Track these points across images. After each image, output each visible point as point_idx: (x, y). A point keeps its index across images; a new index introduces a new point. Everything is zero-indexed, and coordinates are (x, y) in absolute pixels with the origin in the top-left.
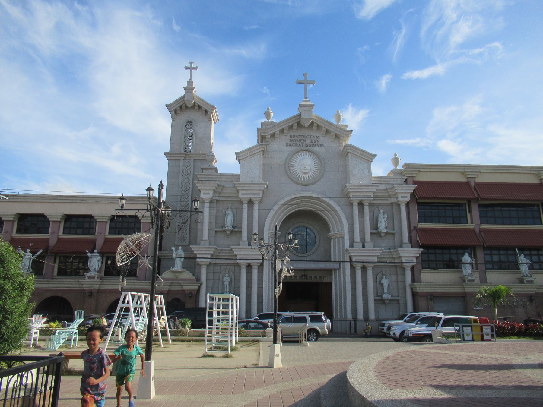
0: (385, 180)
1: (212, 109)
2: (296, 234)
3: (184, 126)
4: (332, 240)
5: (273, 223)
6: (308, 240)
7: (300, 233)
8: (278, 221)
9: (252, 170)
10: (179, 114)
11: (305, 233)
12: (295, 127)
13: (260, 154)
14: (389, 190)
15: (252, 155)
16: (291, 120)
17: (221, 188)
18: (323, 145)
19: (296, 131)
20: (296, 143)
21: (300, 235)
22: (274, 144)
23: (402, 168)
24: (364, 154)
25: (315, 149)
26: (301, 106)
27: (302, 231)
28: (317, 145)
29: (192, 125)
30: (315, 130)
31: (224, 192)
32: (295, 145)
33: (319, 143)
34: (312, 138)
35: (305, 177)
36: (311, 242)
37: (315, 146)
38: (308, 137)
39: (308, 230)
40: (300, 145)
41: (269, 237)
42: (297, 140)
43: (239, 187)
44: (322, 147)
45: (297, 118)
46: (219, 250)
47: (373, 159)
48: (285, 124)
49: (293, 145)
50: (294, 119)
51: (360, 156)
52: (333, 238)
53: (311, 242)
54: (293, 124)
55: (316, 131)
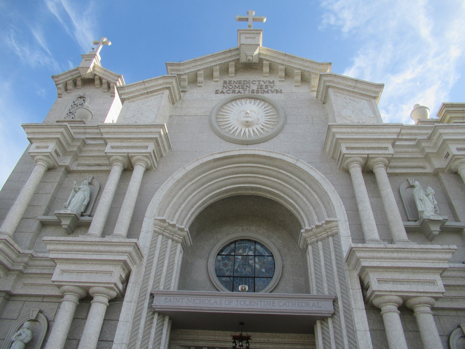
0: (409, 131)
1: (116, 78)
2: (233, 254)
3: (72, 101)
4: (310, 247)
5: (171, 206)
6: (257, 266)
7: (241, 251)
8: (183, 206)
9: (142, 114)
10: (71, 90)
11: (251, 253)
12: (232, 69)
13: (163, 93)
14: (423, 144)
15: (148, 93)
16: (224, 56)
17: (79, 144)
18: (281, 90)
19: (234, 75)
20: (233, 89)
21: (240, 257)
22: (195, 91)
23: (437, 118)
24: (359, 85)
25: (266, 95)
26: (241, 32)
27: (244, 249)
28: (269, 91)
29: (84, 100)
30: (266, 73)
31: (86, 155)
32: (231, 92)
33: (273, 89)
34: (262, 83)
35: (247, 131)
36: (263, 270)
37: (267, 92)
38: (254, 82)
39: (258, 247)
40: (239, 92)
41: (155, 232)
42: (235, 86)
43: (107, 133)
44: (280, 94)
45: (234, 53)
46: (25, 255)
47: (378, 93)
48: (214, 61)
49: (228, 92)
50: (230, 55)
51: (352, 90)
52: (312, 244)
53: (263, 270)
54: (228, 63)
55: (268, 75)
